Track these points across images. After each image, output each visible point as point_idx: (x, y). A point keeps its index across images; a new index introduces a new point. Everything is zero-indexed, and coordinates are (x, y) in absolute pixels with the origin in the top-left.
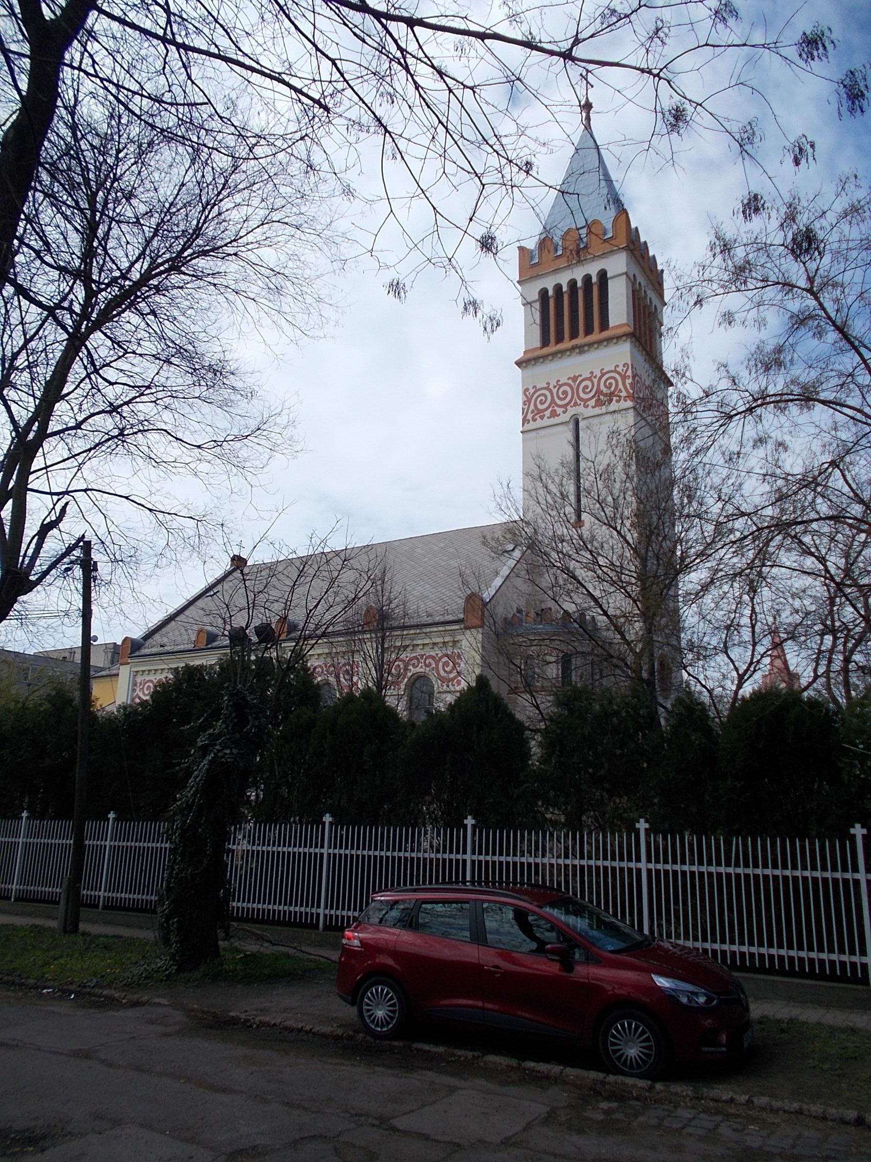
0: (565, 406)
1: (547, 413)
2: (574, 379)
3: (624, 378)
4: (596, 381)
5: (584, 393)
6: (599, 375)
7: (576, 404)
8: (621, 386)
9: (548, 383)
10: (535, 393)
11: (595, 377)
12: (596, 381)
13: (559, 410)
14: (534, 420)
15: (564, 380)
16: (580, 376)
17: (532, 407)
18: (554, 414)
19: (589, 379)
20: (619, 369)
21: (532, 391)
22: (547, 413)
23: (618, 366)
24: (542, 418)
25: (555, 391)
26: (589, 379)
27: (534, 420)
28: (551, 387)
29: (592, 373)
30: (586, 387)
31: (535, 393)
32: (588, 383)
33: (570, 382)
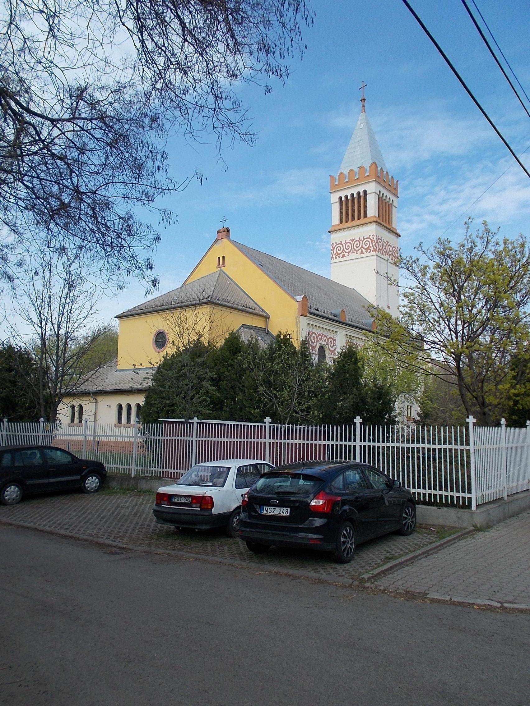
0: (348, 252)
1: (341, 255)
3: (372, 241)
4: (361, 242)
5: (357, 247)
7: (353, 252)
8: (371, 245)
12: (361, 242)
13: (346, 254)
17: (335, 252)
19: (358, 241)
20: (371, 237)
21: (335, 244)
22: (341, 255)
24: (339, 257)
25: (344, 245)
26: (358, 241)
27: (336, 258)
30: (357, 244)
32: (358, 242)
33: (351, 242)
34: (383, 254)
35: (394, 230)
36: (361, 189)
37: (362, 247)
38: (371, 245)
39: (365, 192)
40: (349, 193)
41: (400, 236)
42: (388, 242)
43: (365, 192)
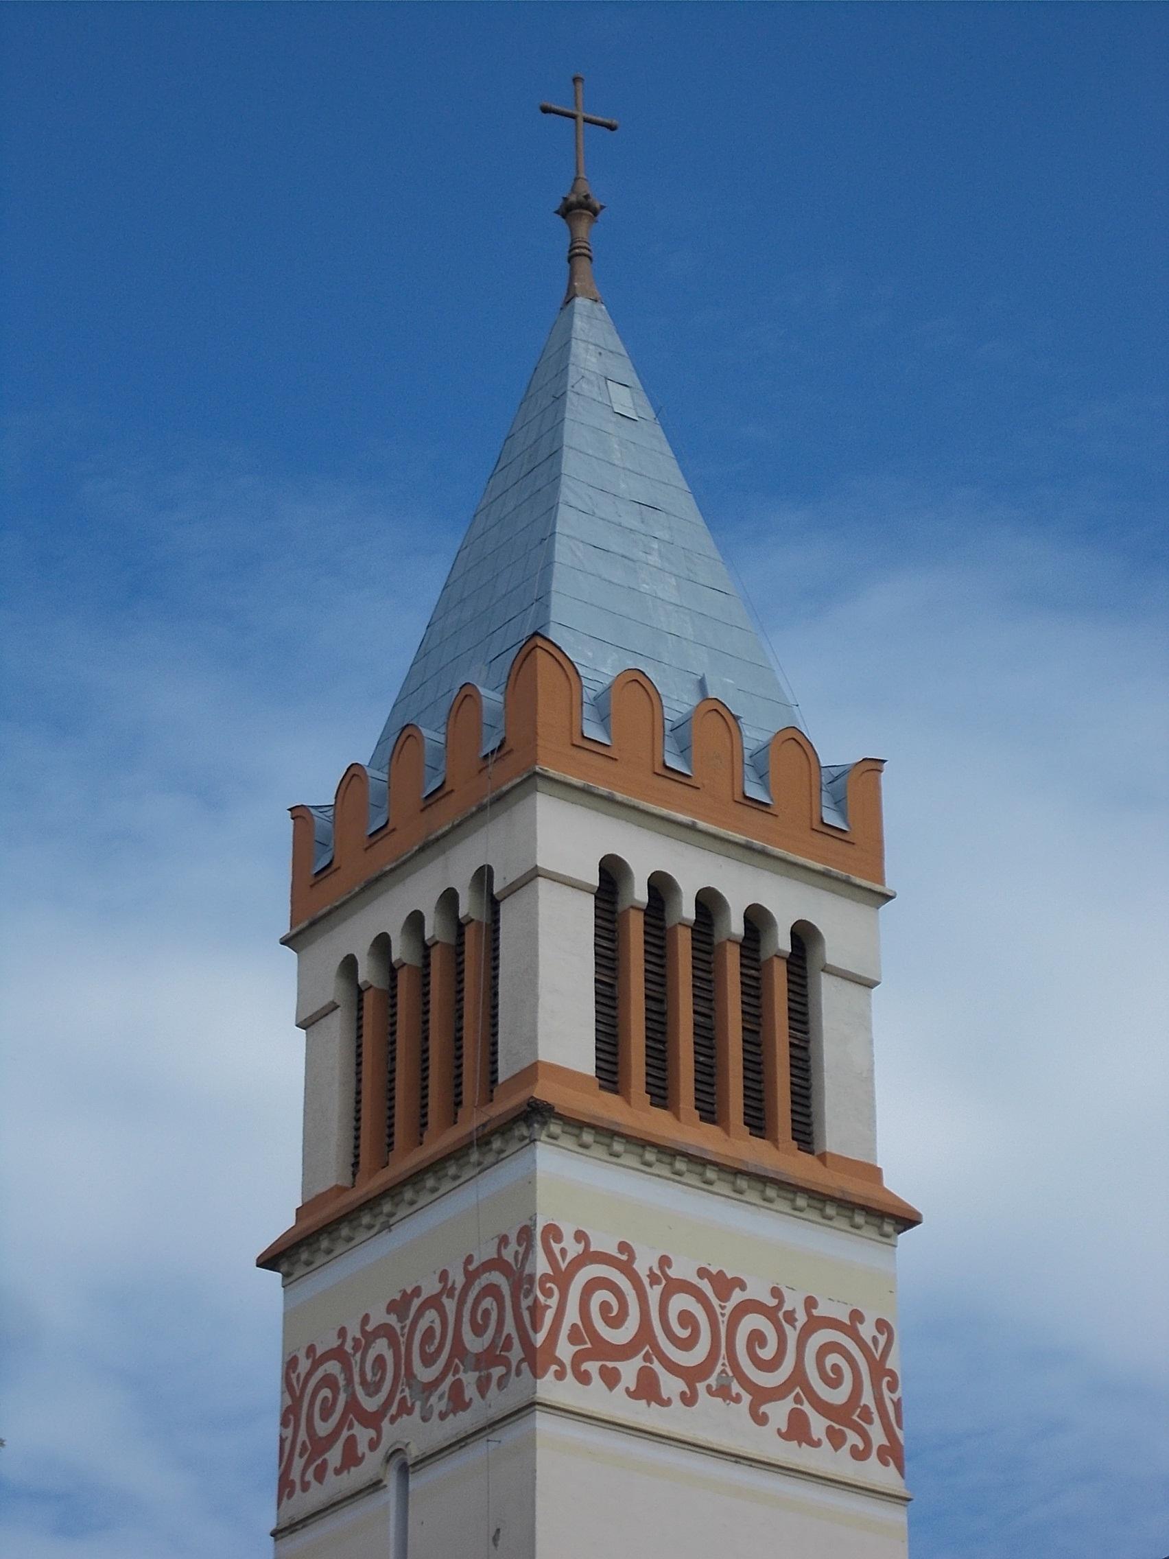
1: (334, 1456)
2: (398, 1307)
6: (458, 1278)
7: (404, 1409)
9: (342, 1333)
10: (309, 1374)
11: (450, 1293)
12: (450, 1305)
14: (305, 1487)
15: (380, 1316)
16: (417, 1291)
17: (303, 1435)
18: (351, 1458)
20: (508, 1255)
22: (334, 1456)
23: (504, 1240)
26: (434, 1302)
28: (348, 1347)
29: (444, 1276)
31: (309, 1374)
33: (392, 1320)
34: (647, 1389)
35: (856, 1189)
36: (455, 869)
37: (459, 1348)
38: (510, 1327)
39: (484, 876)
40: (386, 915)
41: (906, 1220)
42: (724, 1285)
43: (484, 876)
